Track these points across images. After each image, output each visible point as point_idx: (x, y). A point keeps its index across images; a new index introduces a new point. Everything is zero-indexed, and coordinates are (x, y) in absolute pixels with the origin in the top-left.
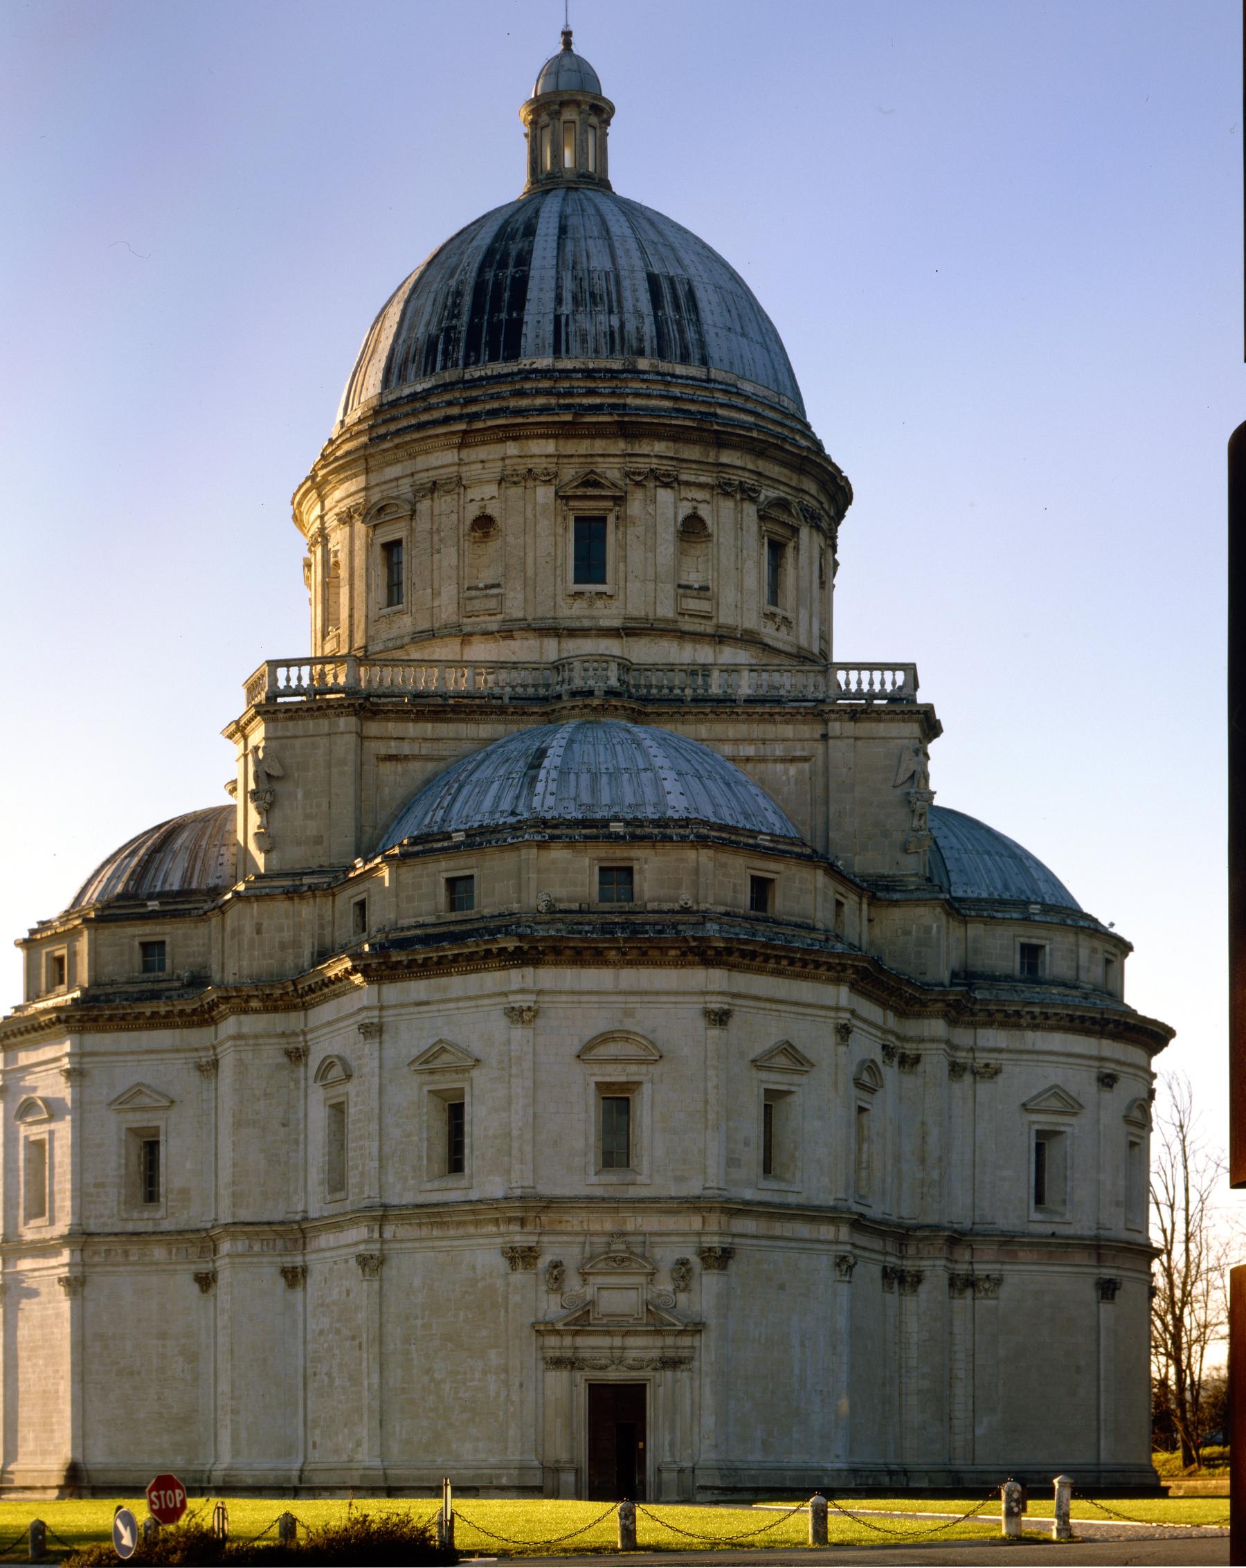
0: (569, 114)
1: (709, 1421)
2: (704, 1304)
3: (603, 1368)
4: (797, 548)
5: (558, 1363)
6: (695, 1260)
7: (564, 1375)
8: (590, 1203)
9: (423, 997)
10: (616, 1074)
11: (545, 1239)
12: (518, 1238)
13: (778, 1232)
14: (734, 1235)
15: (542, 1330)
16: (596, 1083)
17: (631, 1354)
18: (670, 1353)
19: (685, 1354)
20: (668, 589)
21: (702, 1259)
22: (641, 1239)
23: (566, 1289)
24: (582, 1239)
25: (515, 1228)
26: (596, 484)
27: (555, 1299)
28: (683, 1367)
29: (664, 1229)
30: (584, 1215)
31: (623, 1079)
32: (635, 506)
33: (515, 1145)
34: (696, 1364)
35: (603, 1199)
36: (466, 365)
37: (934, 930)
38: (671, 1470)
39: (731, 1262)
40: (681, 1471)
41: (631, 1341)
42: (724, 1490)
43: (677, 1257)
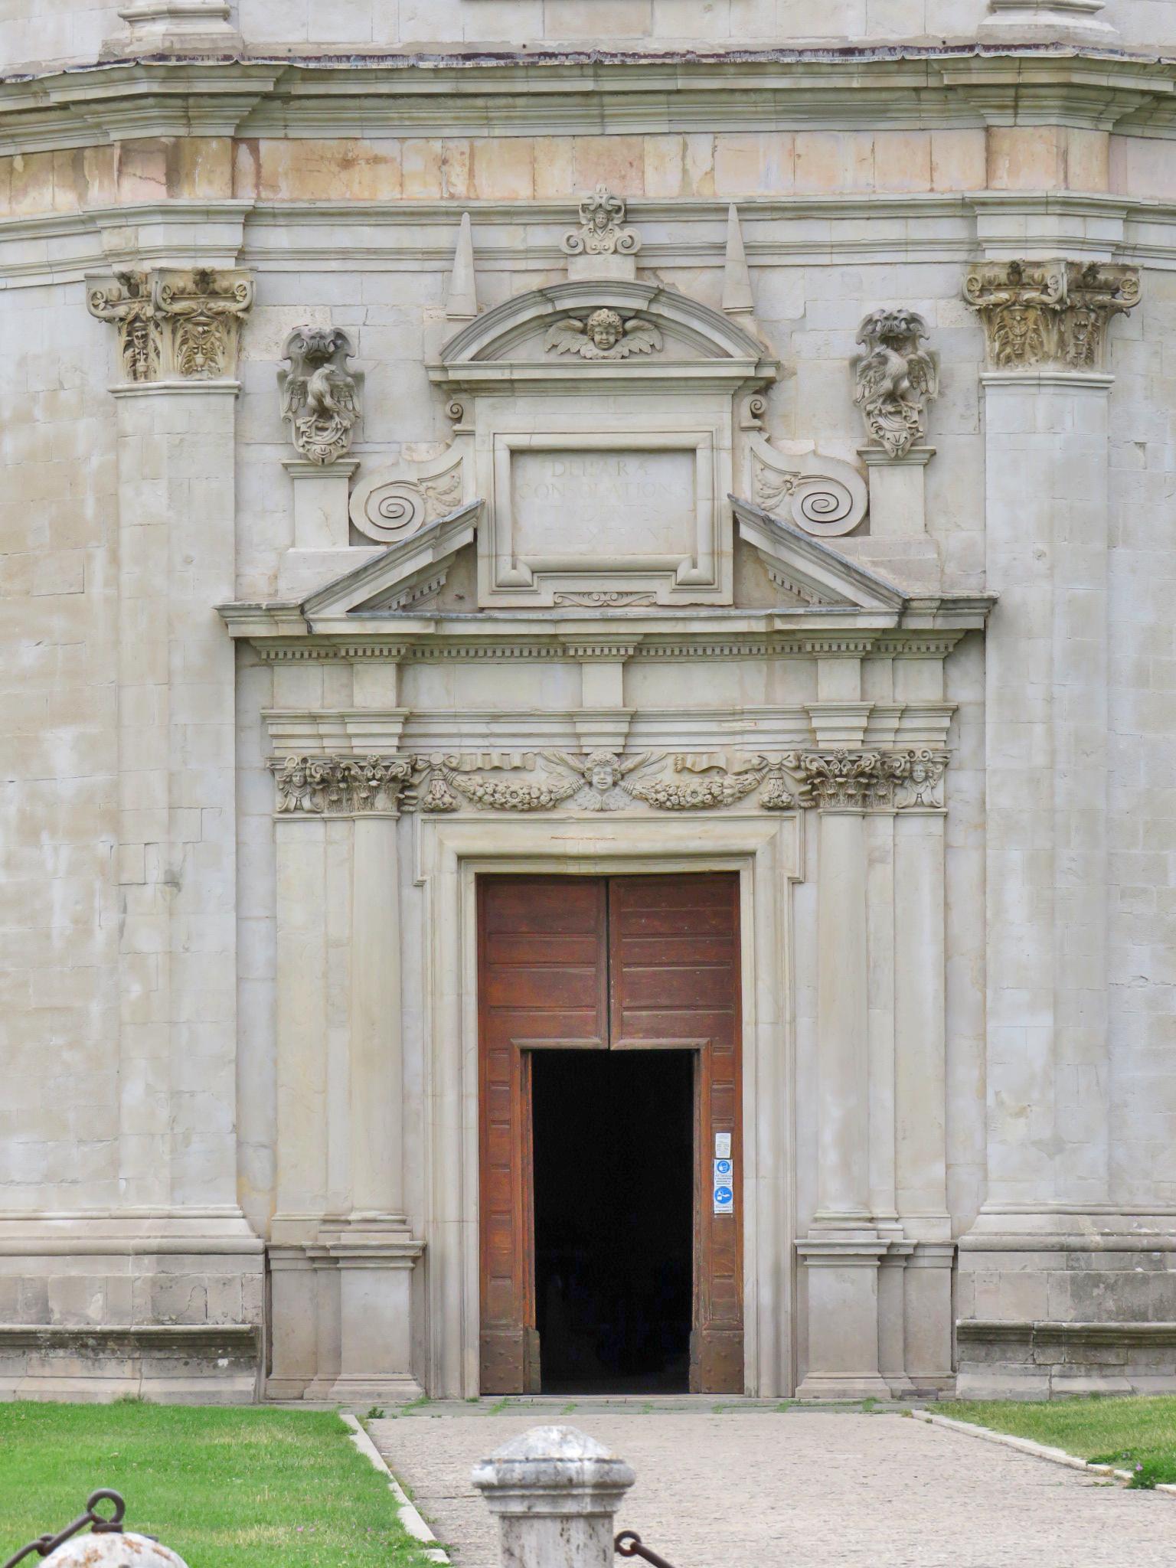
1: (1023, 1033)
2: (996, 513)
3: (531, 807)
5: (334, 785)
6: (946, 322)
7: (367, 835)
11: (275, 237)
12: (153, 236)
14: (1133, 213)
18: (840, 737)
19: (917, 738)
21: (986, 313)
22: (705, 232)
23: (379, 466)
24: (437, 236)
25: (142, 189)
28: (905, 796)
29: (813, 190)
34: (963, 781)
35: (540, 61)
38: (840, 1258)
39: (1126, 327)
40: (890, 1259)
41: (664, 687)
42: (1088, 1344)
43: (872, 307)
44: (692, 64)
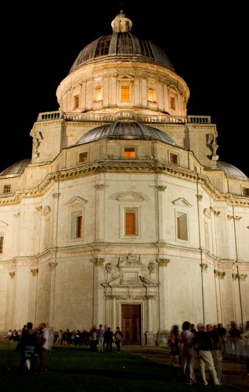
0: (121, 23)
3: (126, 299)
4: (178, 98)
5: (111, 297)
8: (121, 244)
9: (71, 185)
10: (130, 205)
11: (107, 256)
13: (183, 256)
14: (169, 255)
15: (106, 285)
16: (124, 208)
17: (136, 294)
20: (146, 101)
26: (126, 78)
27: (109, 276)
30: (119, 248)
31: (132, 206)
32: (137, 82)
33: (97, 226)
36: (95, 57)
37: (221, 180)
41: (136, 290)
44: (137, 244)
